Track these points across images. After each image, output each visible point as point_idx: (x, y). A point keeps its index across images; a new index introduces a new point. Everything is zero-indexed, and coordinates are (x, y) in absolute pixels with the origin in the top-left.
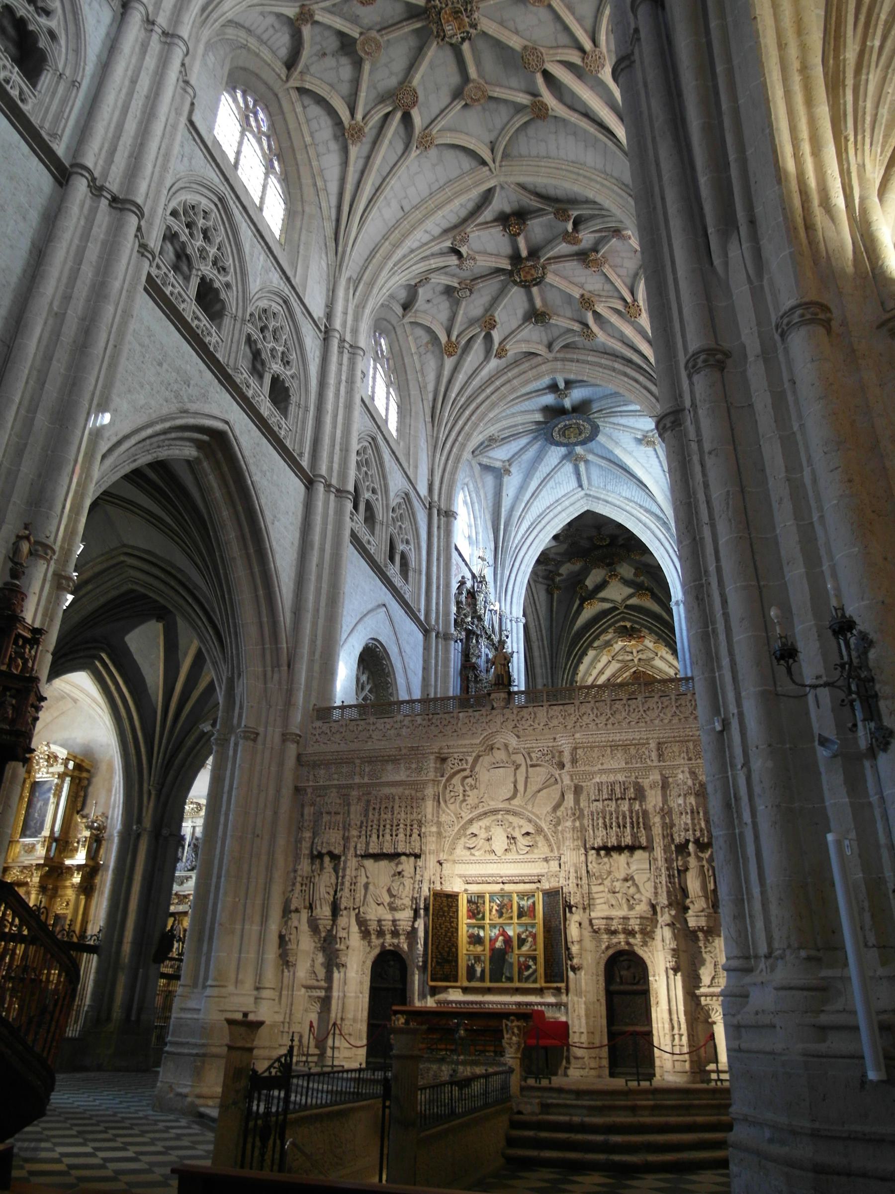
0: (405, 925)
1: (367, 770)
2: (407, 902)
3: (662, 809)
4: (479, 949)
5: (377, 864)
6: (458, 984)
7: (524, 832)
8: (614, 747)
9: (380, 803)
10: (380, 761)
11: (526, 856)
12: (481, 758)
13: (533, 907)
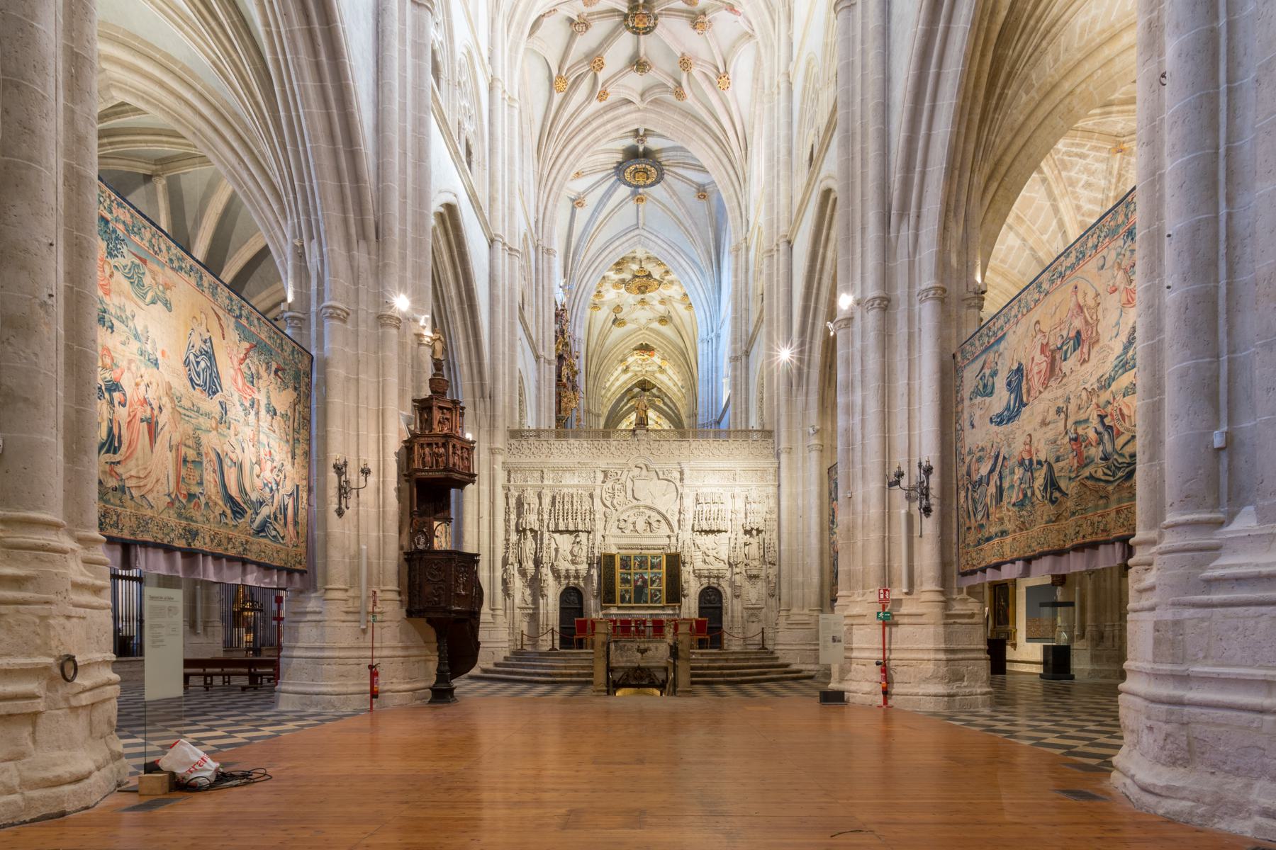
4: (627, 587)
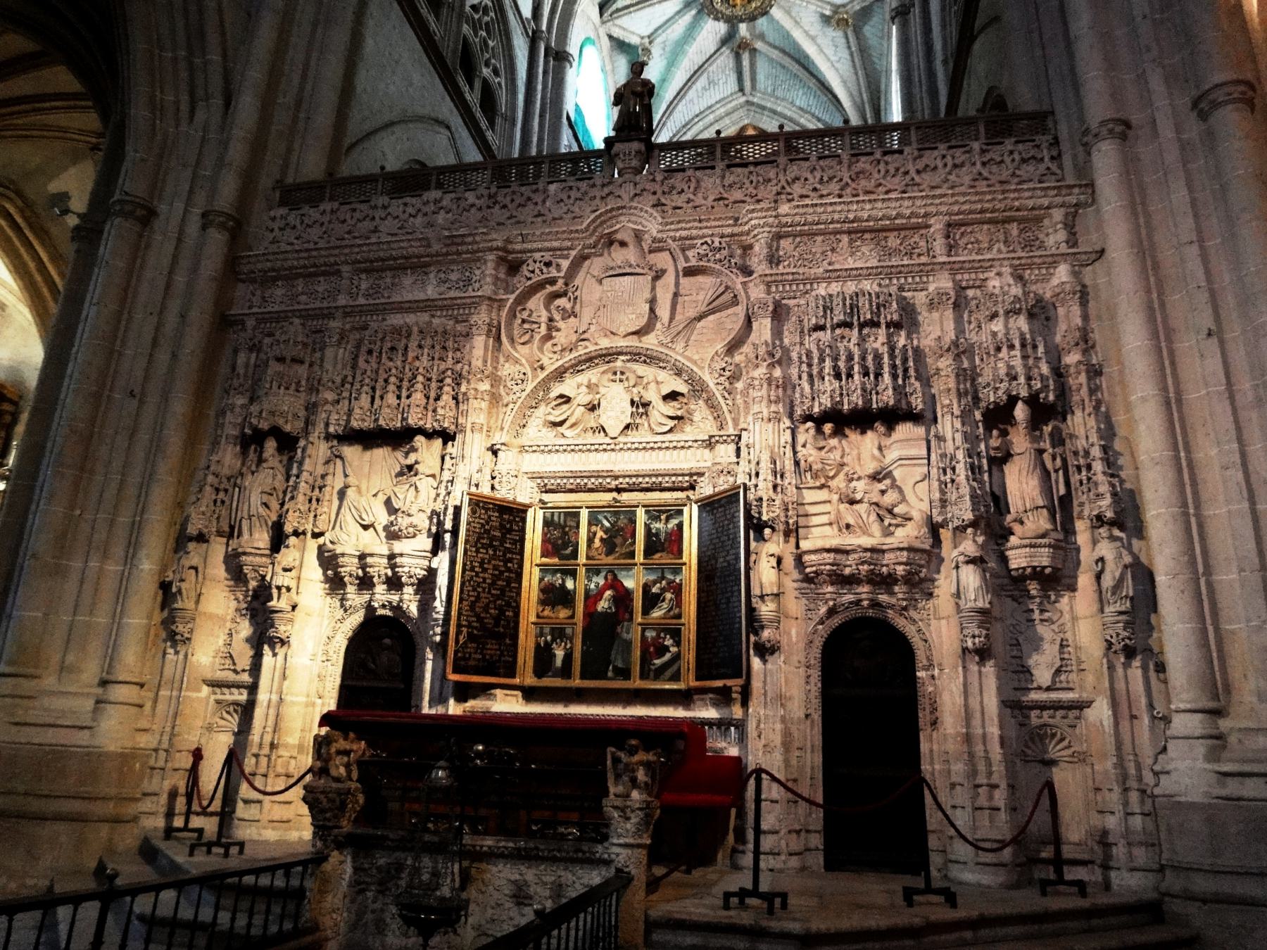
0: (413, 567)
1: (364, 286)
2: (422, 521)
3: (955, 344)
4: (563, 613)
5: (368, 453)
6: (517, 681)
7: (665, 391)
8: (857, 232)
9: (382, 340)
10: (391, 269)
11: (669, 437)
12: (587, 263)
13: (677, 536)
